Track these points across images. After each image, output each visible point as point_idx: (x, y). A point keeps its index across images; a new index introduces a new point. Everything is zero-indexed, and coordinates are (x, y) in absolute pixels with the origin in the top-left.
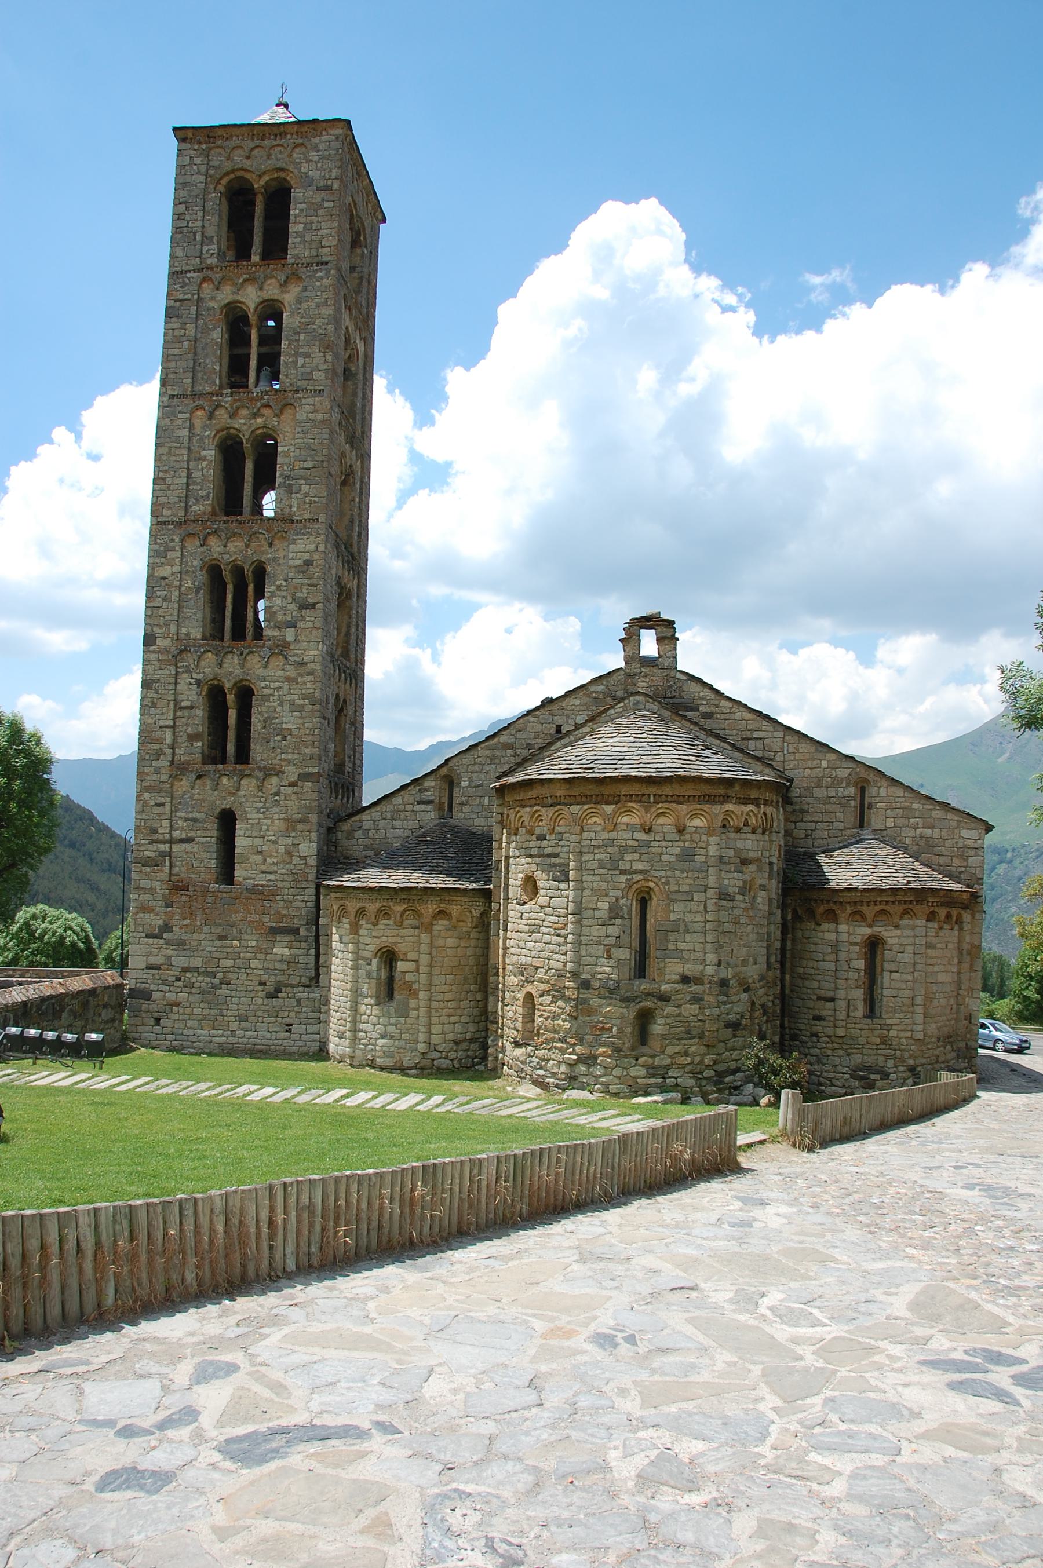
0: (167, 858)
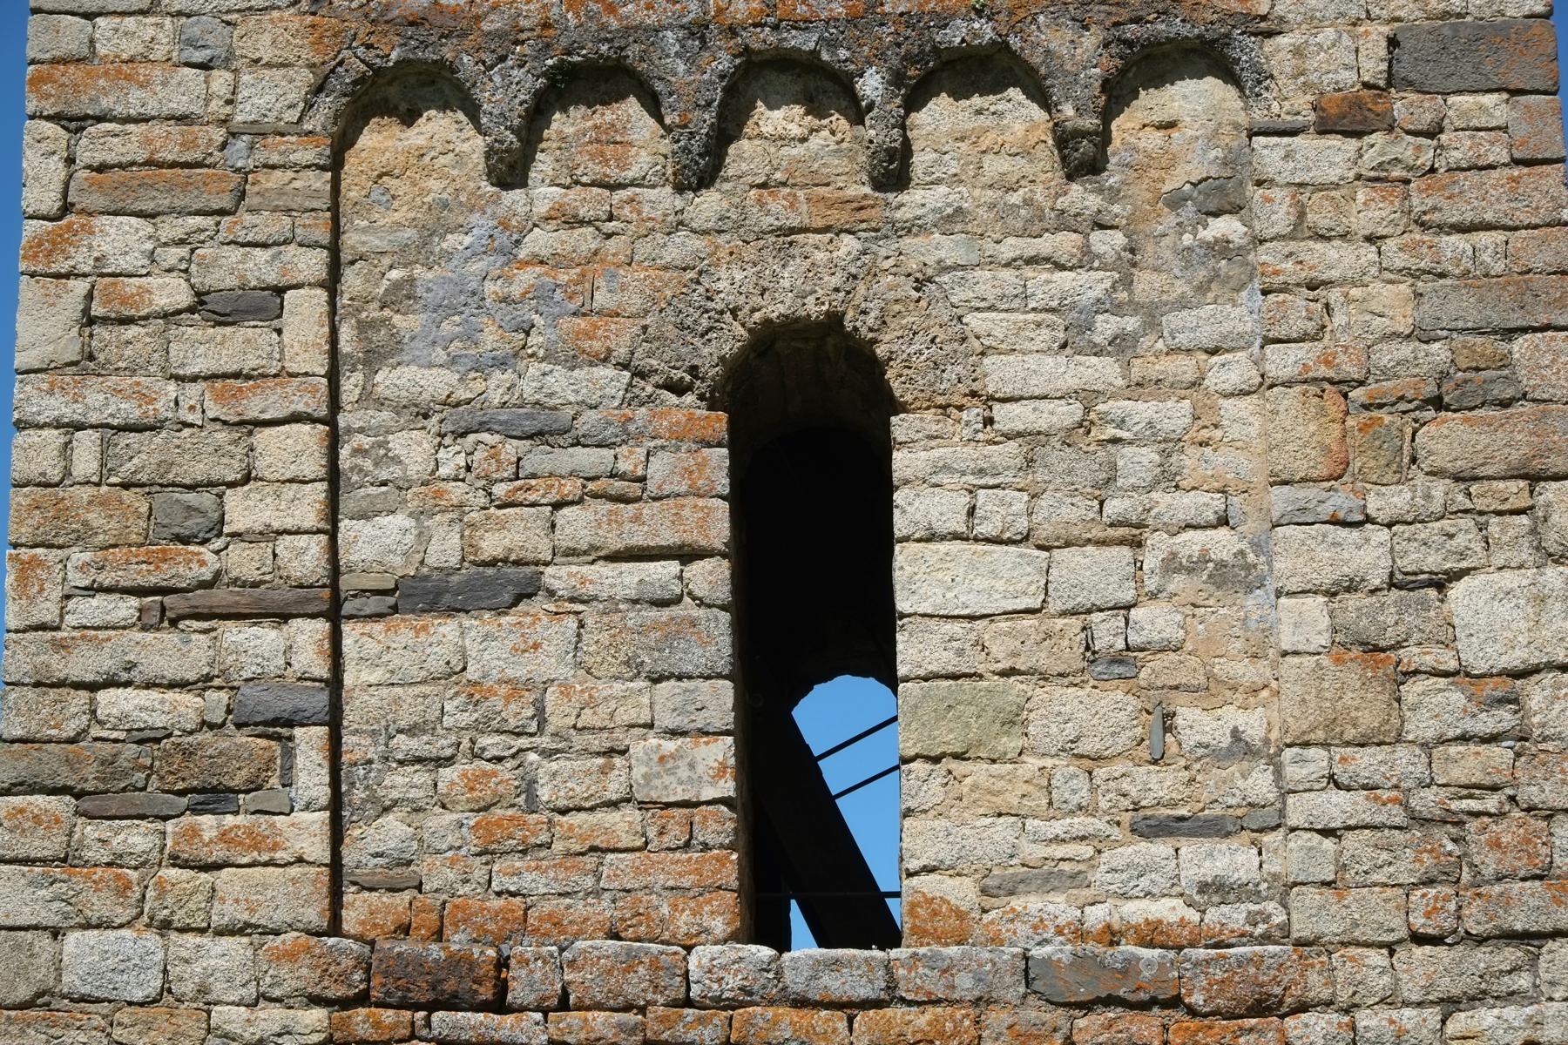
0: (310, 741)
